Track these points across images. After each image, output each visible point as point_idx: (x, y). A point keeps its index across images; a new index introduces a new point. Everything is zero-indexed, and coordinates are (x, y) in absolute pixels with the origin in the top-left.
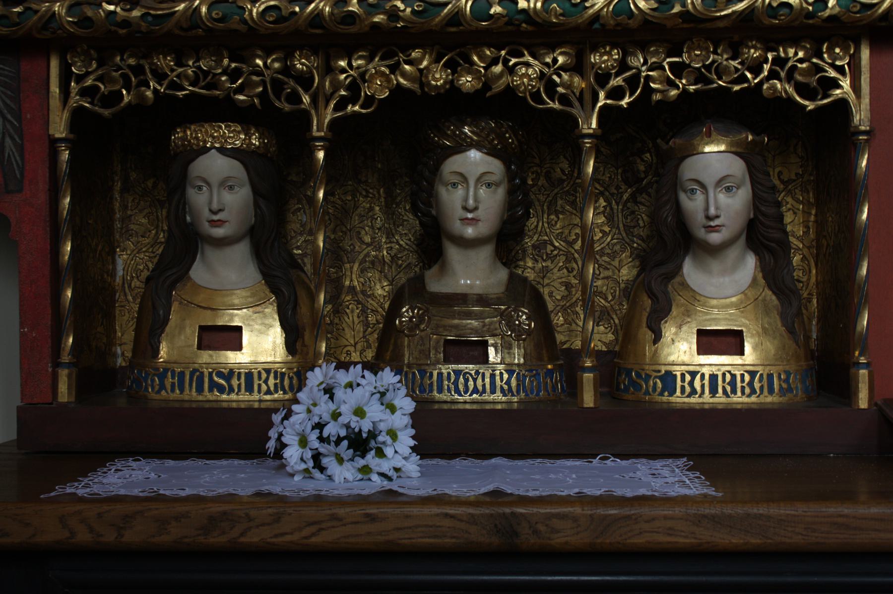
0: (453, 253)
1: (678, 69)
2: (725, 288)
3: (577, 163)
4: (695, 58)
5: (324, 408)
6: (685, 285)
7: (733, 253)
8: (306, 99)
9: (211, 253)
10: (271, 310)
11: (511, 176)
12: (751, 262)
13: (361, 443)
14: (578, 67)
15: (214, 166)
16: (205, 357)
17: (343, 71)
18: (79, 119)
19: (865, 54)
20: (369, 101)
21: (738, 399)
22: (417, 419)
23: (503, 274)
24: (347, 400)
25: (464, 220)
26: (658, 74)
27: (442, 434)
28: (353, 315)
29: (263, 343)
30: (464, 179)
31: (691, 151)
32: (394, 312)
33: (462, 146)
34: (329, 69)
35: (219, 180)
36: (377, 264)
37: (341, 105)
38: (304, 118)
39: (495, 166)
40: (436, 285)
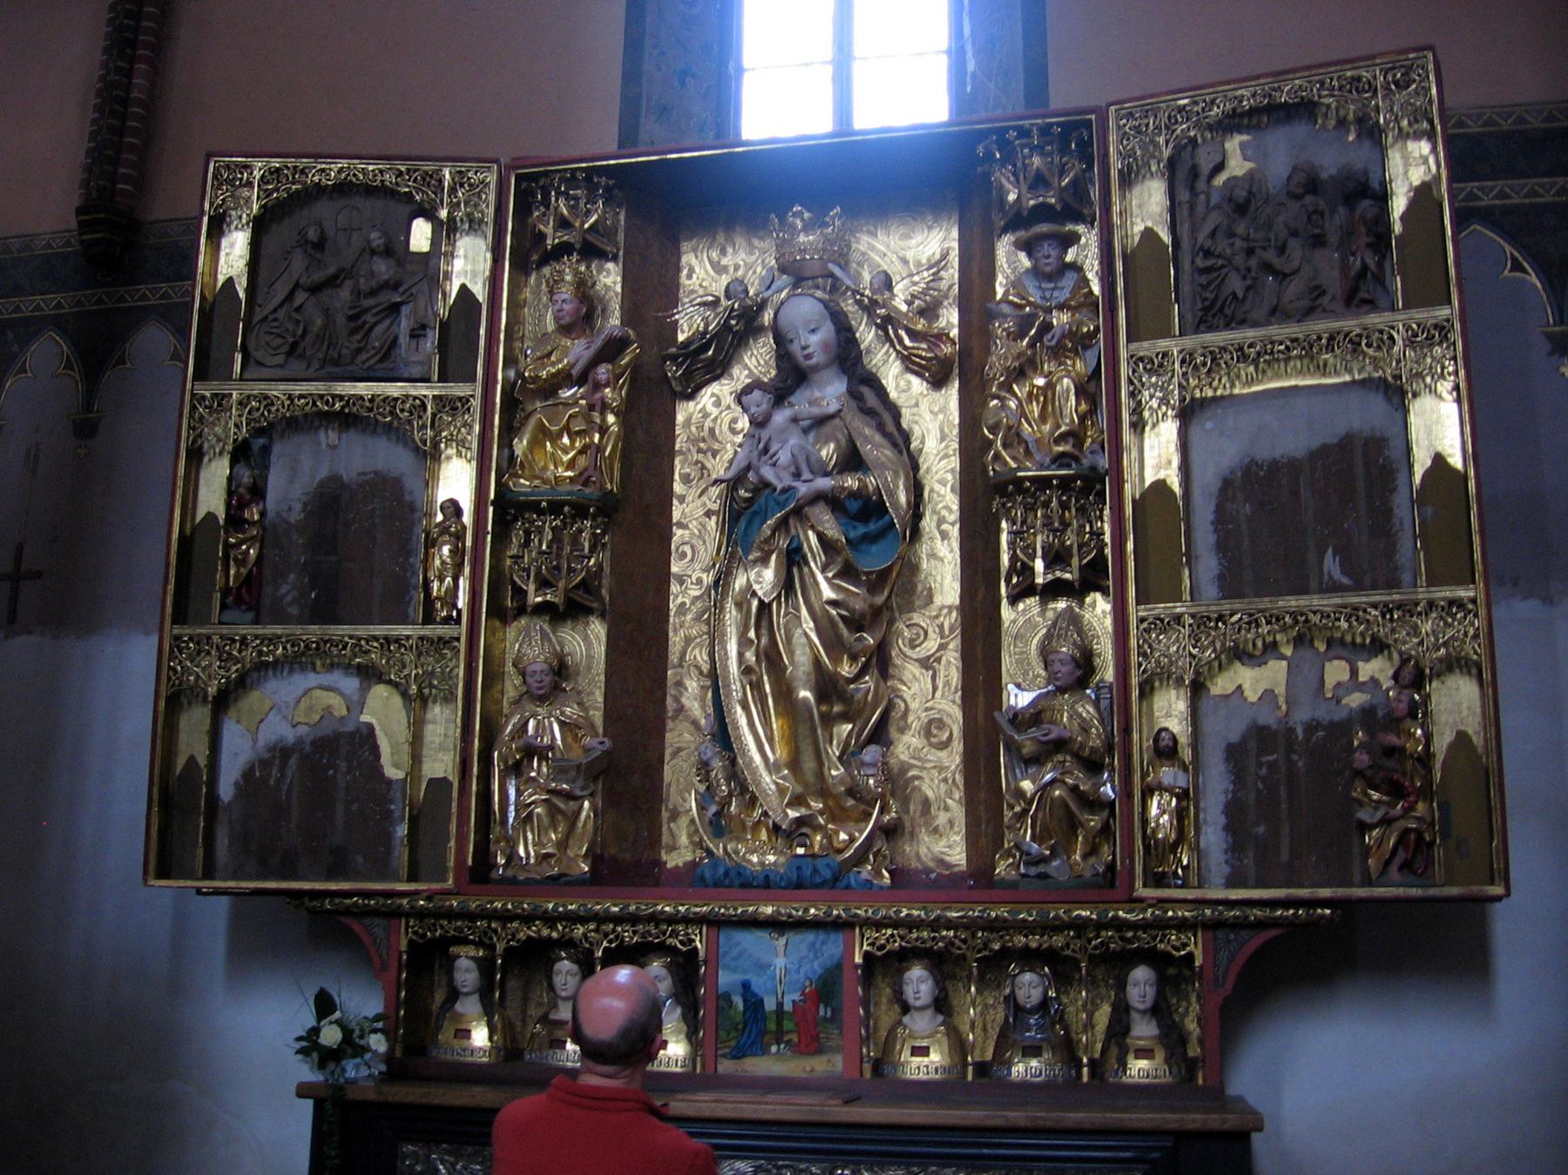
0: (560, 1003)
1: (635, 933)
14: (597, 931)
16: (455, 1042)
18: (411, 943)
26: (629, 936)
35: (466, 971)
40: (553, 1016)
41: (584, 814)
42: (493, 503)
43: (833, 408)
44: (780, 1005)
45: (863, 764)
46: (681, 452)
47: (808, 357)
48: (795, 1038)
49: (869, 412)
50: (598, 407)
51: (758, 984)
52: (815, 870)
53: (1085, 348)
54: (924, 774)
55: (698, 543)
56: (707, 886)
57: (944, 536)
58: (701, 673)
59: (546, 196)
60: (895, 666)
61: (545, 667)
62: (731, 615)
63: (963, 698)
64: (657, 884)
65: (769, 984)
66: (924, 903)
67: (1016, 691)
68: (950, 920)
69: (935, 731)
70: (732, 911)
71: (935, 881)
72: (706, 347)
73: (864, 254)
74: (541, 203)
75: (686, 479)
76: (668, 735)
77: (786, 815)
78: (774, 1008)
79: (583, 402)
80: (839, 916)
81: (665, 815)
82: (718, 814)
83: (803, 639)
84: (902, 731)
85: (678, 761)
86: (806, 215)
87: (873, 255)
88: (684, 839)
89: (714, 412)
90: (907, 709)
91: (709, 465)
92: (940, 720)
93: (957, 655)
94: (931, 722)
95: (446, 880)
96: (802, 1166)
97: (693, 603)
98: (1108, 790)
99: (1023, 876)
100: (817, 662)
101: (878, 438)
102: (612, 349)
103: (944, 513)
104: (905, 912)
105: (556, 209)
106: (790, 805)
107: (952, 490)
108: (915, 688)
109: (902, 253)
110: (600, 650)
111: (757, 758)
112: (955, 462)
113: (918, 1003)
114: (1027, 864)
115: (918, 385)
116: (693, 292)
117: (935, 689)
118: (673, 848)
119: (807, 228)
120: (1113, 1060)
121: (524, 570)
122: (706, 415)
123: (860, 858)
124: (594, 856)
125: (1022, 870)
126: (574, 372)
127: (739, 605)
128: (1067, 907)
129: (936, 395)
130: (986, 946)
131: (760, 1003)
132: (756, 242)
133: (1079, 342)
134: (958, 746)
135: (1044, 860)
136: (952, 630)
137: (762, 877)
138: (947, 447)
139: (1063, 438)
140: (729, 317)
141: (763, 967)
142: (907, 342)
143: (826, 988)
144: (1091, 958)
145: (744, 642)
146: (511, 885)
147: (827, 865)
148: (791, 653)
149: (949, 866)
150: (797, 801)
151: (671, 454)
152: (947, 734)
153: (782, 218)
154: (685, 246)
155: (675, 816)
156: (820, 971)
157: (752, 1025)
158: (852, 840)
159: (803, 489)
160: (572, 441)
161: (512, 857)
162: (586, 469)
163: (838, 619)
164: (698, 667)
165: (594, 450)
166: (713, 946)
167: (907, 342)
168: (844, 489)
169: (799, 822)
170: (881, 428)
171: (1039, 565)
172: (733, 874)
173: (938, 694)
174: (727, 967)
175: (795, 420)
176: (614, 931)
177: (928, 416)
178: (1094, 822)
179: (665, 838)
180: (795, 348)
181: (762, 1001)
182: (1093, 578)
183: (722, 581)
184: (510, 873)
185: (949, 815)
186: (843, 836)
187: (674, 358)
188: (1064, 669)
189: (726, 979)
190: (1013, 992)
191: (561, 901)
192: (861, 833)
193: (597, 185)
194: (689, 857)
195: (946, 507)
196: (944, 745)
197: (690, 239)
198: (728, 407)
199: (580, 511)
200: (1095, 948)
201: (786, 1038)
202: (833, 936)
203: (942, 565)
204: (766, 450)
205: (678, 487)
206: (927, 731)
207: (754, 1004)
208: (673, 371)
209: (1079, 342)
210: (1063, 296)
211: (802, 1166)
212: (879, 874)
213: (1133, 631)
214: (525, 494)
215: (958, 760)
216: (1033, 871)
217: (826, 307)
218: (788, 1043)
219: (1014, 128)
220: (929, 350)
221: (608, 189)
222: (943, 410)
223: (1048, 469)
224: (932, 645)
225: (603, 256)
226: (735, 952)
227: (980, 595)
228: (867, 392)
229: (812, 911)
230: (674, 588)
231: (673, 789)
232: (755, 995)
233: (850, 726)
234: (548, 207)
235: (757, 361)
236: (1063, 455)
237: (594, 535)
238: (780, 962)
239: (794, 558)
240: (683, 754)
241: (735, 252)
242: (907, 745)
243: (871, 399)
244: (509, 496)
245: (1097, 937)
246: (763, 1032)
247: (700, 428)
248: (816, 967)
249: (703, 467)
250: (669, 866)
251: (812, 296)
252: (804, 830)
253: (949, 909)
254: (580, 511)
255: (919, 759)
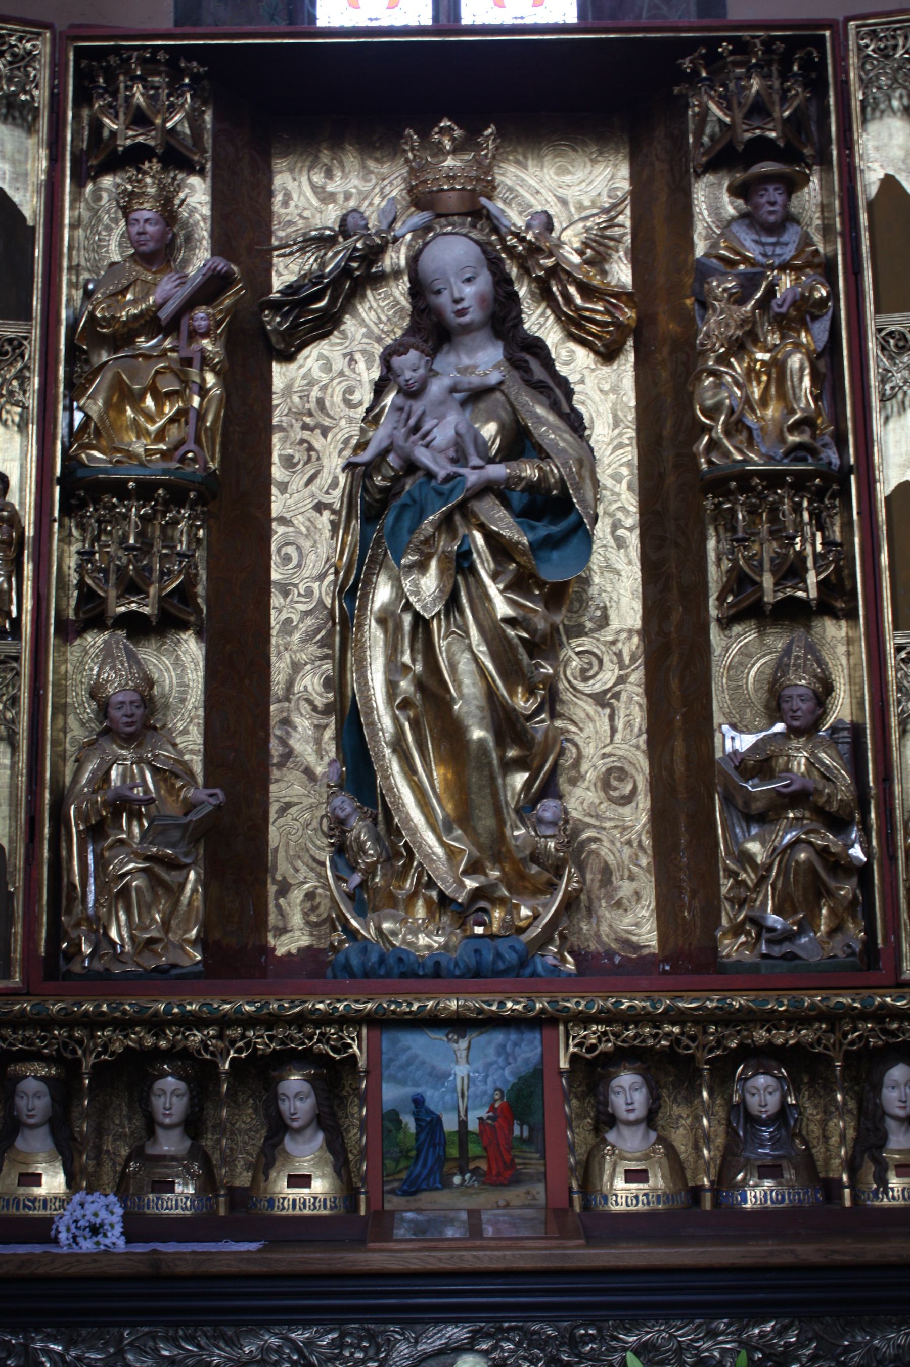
0: (160, 1132)
2: (307, 1154)
3: (219, 1085)
4: (279, 1032)
5: (79, 1213)
6: (284, 1151)
7: (309, 1132)
8: (80, 1052)
9: (27, 1132)
10: (59, 1165)
11: (191, 1090)
12: (320, 1137)
13: (95, 1230)
14: (220, 1036)
15: (31, 1086)
17: (99, 1037)
19: (364, 1031)
20: (113, 1053)
21: (307, 1212)
22: (126, 1218)
23: (188, 1143)
24: (90, 1209)
25: (165, 1115)
26: (262, 1041)
27: (137, 1227)
28: (107, 1167)
29: (53, 1182)
30: (164, 1092)
31: (283, 1079)
32: (127, 1165)
33: (164, 1075)
34: (92, 1037)
36: (121, 1137)
37: (98, 1055)
38: (79, 1062)
39: (182, 1086)
40: (151, 1150)
41: (189, 887)
42: (60, 481)
43: (494, 378)
44: (463, 1124)
45: (541, 821)
46: (281, 428)
47: (461, 313)
48: (484, 1166)
49: (538, 387)
50: (197, 362)
51: (434, 1099)
52: (498, 955)
53: (815, 318)
54: (603, 836)
55: (306, 545)
56: (352, 975)
57: (620, 543)
58: (315, 708)
59: (111, 79)
60: (562, 702)
61: (136, 697)
62: (374, 635)
63: (649, 742)
64: (264, 976)
65: (448, 1097)
66: (648, 992)
67: (733, 733)
68: (682, 1012)
69: (614, 783)
70: (405, 1007)
71: (620, 965)
72: (318, 296)
73: (511, 189)
74: (106, 90)
75: (289, 463)
76: (273, 788)
77: (463, 885)
78: (456, 1128)
79: (175, 355)
80: (543, 1010)
81: (272, 889)
82: (362, 885)
83: (467, 667)
84: (573, 782)
85: (287, 819)
86: (457, 133)
87: (522, 191)
88: (297, 919)
89: (325, 378)
90: (580, 757)
91: (316, 445)
92: (621, 769)
93: (640, 690)
94: (609, 771)
95: (8, 976)
96: (536, 1327)
97: (302, 620)
98: (857, 852)
99: (765, 956)
100: (491, 693)
101: (551, 418)
102: (212, 287)
103: (620, 515)
104: (626, 1004)
105: (128, 99)
106: (465, 873)
107: (629, 488)
108: (589, 729)
109: (561, 192)
110: (196, 677)
111: (417, 816)
112: (630, 454)
113: (632, 1117)
114: (769, 942)
115: (583, 356)
116: (290, 223)
117: (613, 730)
118: (283, 930)
119: (454, 151)
120: (870, 1178)
121: (100, 570)
122: (311, 383)
123: (545, 939)
124: (201, 942)
125: (764, 949)
126: (164, 315)
127: (382, 621)
128: (824, 993)
129: (605, 370)
130: (719, 1043)
131: (437, 1122)
132: (371, 164)
133: (804, 311)
134: (643, 802)
135: (788, 937)
136: (633, 659)
137: (430, 963)
138: (620, 435)
139: (796, 427)
140: (351, 259)
141: (440, 1077)
142: (578, 301)
143: (521, 1100)
144: (848, 1057)
145: (394, 669)
146: (101, 981)
147: (512, 948)
148: (458, 684)
149: (637, 947)
150: (474, 869)
151: (267, 429)
152: (629, 787)
153: (424, 135)
154: (279, 164)
155: (284, 889)
156: (512, 1080)
157: (428, 1153)
158: (536, 917)
159: (472, 477)
160: (159, 404)
161: (102, 940)
162: (182, 442)
163: (516, 641)
164: (310, 702)
165: (192, 416)
166: (374, 1053)
167: (578, 301)
168: (521, 479)
169: (476, 894)
170: (554, 407)
171: (768, 581)
172: (391, 961)
173: (618, 737)
174: (394, 1079)
175: (453, 390)
176: (243, 1036)
177: (597, 396)
178: (846, 890)
179: (273, 918)
180: (444, 300)
181: (439, 1120)
182: (836, 599)
183: (352, 591)
184: (98, 966)
185: (634, 885)
186: (525, 912)
187: (276, 306)
188: (804, 706)
189: (391, 1094)
190: (743, 1100)
191: (176, 999)
192: (547, 906)
193: (182, 73)
194: (305, 941)
195: (622, 509)
196: (627, 800)
197: (285, 154)
198: (341, 374)
199: (177, 495)
200: (852, 1043)
201: (472, 1166)
202: (528, 1036)
203: (617, 578)
204: (416, 429)
205: (277, 472)
206: (605, 783)
207: (429, 1124)
208: (273, 322)
209: (804, 311)
210: (788, 252)
211: (536, 1327)
212: (564, 960)
213: (891, 662)
214: (104, 471)
215: (644, 818)
216: (777, 951)
217: (484, 252)
218: (475, 1171)
219: (729, 40)
220: (607, 312)
221: (195, 78)
222: (615, 389)
223: (779, 462)
224: (607, 678)
225: (191, 168)
226: (404, 1058)
227: (675, 617)
228: (535, 365)
229: (509, 1005)
230: (276, 600)
231: (281, 855)
232: (430, 1112)
233: (526, 775)
234: (115, 94)
235: (378, 315)
236: (799, 446)
237: (191, 526)
238: (461, 1070)
239: (461, 565)
240: (293, 810)
241: (345, 176)
242: (581, 799)
243: (539, 372)
244: (80, 473)
245: (855, 1029)
246: (442, 1159)
247: (305, 398)
248: (508, 1076)
249: (311, 448)
250: (280, 952)
251: (466, 235)
252: (482, 904)
253: (681, 998)
254: (177, 495)
255: (597, 817)
